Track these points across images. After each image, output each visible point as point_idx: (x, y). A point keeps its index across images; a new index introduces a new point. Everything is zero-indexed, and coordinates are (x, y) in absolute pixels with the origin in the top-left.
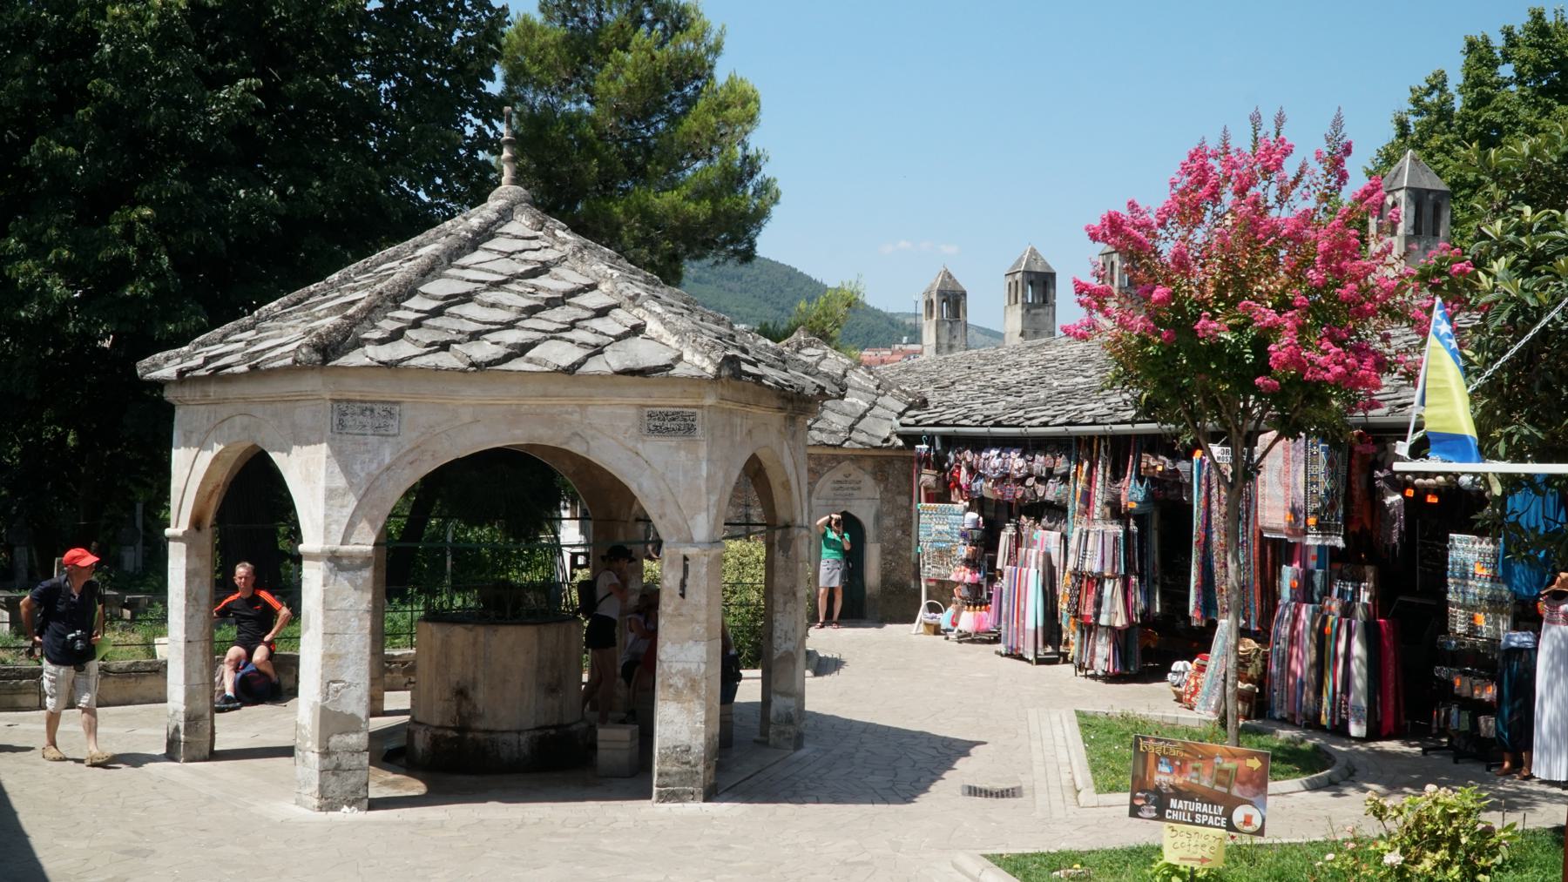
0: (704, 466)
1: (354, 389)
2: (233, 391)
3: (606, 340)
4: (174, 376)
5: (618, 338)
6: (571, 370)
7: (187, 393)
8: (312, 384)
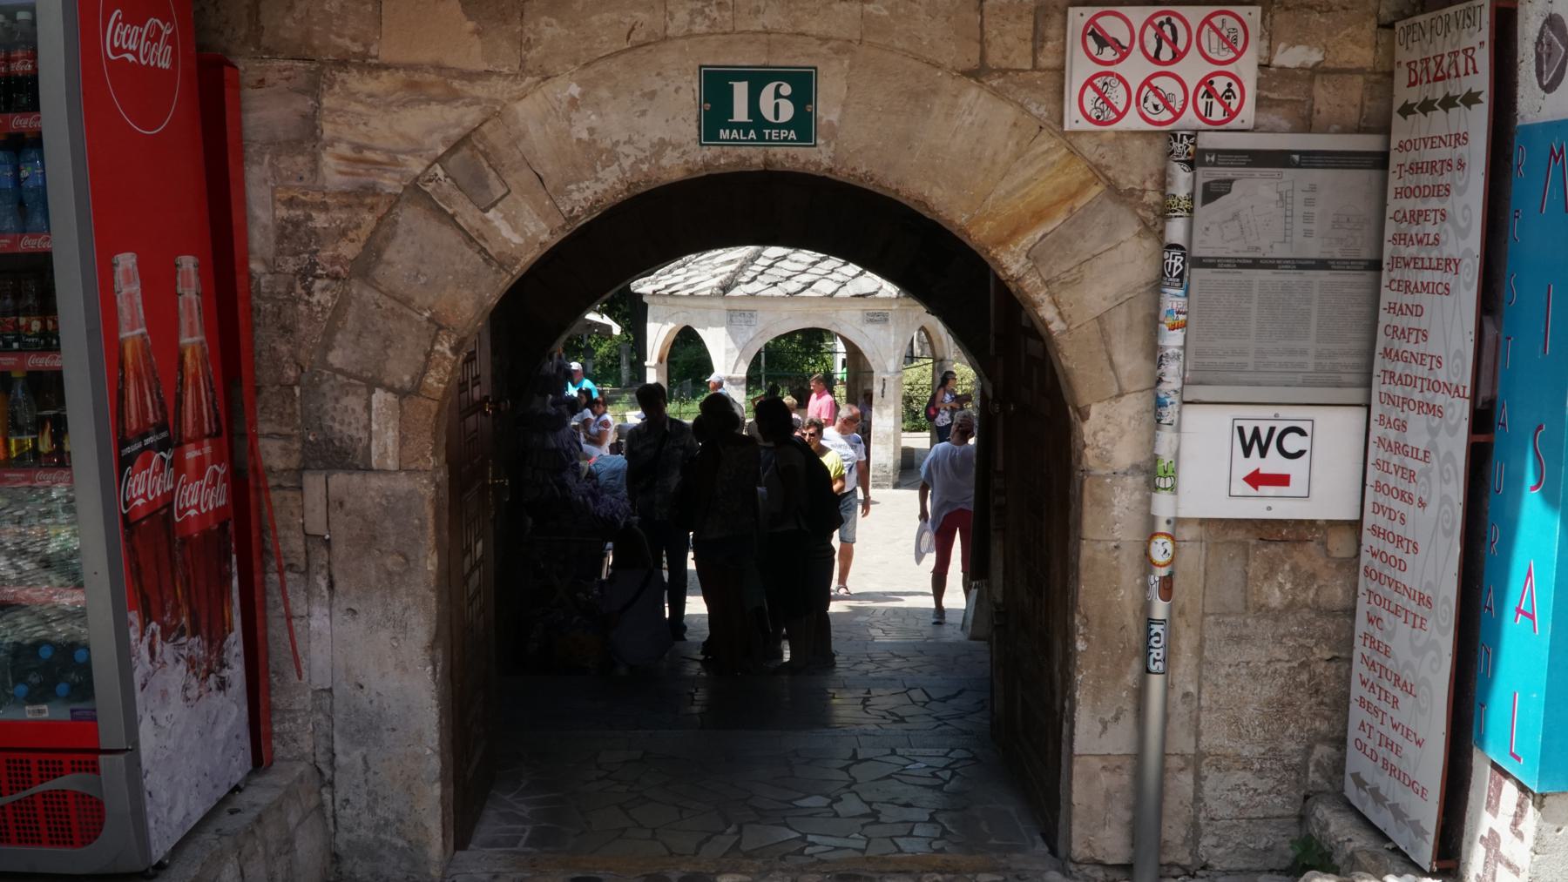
0: (893, 337)
1: (736, 305)
2: (678, 301)
3: (848, 279)
4: (651, 292)
5: (853, 278)
6: (831, 296)
7: (655, 299)
8: (719, 303)
